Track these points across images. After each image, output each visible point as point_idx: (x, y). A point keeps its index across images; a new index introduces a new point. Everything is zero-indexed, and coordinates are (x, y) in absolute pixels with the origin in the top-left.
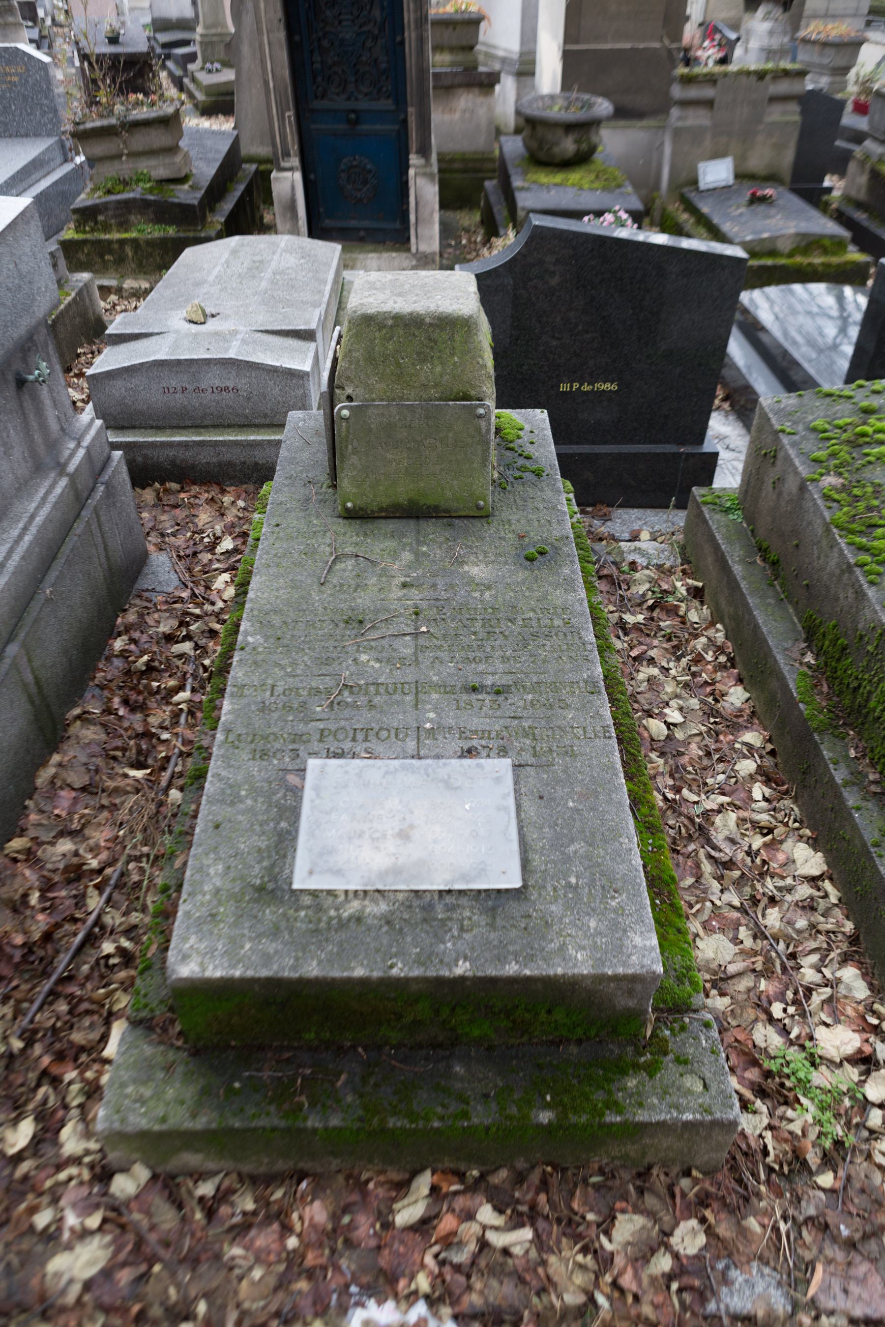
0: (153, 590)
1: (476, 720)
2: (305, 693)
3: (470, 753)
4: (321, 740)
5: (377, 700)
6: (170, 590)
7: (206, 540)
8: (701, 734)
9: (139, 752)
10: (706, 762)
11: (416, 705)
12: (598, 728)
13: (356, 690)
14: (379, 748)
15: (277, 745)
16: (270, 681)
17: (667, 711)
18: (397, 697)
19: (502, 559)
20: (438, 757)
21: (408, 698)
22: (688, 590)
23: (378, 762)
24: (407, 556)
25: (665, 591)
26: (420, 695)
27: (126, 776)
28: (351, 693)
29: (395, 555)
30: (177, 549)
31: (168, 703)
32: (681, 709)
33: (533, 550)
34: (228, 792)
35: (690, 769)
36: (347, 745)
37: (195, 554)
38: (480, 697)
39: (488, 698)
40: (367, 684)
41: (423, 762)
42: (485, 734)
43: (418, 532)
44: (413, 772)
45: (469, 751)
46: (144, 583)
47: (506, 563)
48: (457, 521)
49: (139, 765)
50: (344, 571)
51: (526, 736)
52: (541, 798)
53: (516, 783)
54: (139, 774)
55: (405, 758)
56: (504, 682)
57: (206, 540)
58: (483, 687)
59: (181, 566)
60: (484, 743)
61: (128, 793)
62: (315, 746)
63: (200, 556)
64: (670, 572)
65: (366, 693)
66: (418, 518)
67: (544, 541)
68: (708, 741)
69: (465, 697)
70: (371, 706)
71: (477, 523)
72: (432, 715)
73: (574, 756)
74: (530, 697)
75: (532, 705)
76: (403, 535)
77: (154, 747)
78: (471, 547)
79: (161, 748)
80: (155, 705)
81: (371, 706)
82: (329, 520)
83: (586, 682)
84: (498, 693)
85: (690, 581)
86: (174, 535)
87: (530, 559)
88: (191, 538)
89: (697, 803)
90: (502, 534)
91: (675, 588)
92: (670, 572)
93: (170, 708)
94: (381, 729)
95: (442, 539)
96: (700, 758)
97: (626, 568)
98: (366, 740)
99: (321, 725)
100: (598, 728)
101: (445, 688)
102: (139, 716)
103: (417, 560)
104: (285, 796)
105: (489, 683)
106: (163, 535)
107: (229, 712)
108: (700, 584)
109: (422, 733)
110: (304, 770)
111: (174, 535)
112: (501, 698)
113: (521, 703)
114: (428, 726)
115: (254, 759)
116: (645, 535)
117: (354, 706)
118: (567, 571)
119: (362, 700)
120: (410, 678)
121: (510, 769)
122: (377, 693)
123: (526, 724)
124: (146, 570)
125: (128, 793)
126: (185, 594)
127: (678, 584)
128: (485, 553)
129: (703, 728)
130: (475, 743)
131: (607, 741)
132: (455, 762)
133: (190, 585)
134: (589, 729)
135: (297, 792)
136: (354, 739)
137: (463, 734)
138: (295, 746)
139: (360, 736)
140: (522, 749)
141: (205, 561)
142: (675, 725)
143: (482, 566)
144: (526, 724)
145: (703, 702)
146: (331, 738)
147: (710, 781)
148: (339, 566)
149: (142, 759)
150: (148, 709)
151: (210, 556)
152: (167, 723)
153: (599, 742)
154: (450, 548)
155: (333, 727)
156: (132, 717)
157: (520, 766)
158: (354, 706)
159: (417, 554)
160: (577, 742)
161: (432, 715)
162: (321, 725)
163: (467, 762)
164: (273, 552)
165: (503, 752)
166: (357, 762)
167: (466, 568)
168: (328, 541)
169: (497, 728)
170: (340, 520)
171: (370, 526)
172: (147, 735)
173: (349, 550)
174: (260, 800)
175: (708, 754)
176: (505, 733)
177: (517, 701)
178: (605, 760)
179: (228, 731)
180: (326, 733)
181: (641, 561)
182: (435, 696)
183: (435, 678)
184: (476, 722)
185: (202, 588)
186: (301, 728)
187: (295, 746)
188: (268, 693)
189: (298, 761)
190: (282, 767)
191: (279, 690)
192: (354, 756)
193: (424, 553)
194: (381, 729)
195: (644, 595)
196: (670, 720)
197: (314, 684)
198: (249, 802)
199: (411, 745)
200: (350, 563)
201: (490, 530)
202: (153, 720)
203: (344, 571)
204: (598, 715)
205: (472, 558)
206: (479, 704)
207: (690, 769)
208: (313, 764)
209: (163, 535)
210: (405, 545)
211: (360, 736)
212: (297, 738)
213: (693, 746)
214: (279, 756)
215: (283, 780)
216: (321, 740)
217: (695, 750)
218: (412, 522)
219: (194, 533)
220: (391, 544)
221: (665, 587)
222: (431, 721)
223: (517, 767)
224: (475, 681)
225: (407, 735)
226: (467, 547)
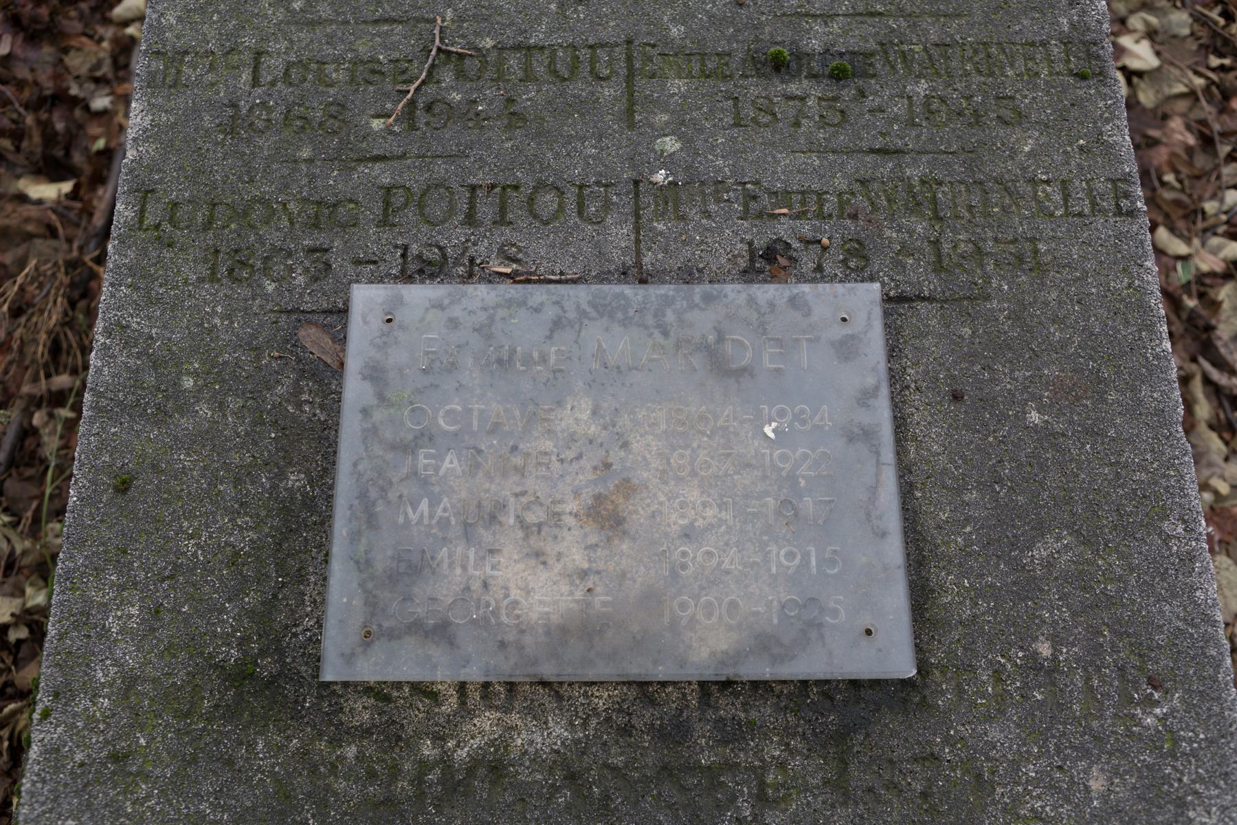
1: (784, 160)
2: (340, 76)
3: (768, 262)
4: (384, 222)
5: (529, 96)
8: (1192, 94)
9: (49, 137)
10: (1201, 161)
11: (630, 112)
12: (1101, 186)
13: (472, 65)
14: (539, 249)
15: (274, 237)
16: (249, 41)
17: (1126, 41)
18: (579, 88)
20: (689, 275)
21: (608, 92)
23: (538, 294)
26: (640, 82)
27: (22, 198)
28: (461, 75)
31: (107, 21)
32: (1150, 34)
34: (150, 379)
35: (1169, 178)
36: (454, 236)
38: (793, 88)
39: (815, 91)
40: (500, 48)
41: (656, 292)
42: (806, 202)
44: (625, 323)
45: (770, 255)
49: (52, 170)
51: (915, 207)
52: (957, 397)
53: (893, 351)
54: (47, 191)
55: (603, 278)
56: (854, 43)
58: (799, 56)
60: (806, 229)
61: (30, 237)
62: (372, 239)
65: (500, 77)
68: (1207, 110)
69: (754, 88)
70: (514, 118)
72: (670, 144)
73: (1039, 269)
74: (922, 87)
75: (930, 113)
77: (81, 127)
79: (94, 129)
80: (77, 26)
81: (514, 118)
83: (1066, 42)
84: (838, 76)
89: (1185, 258)
93: (109, 33)
94: (540, 186)
96: (1189, 150)
98: (502, 220)
99: (383, 175)
100: (1101, 186)
101: (703, 62)
102: (47, 52)
104: (297, 390)
105: (815, 45)
107: (146, 136)
109: (646, 199)
110: (344, 312)
112: (848, 93)
113: (899, 108)
114: (660, 176)
115: (213, 278)
117: (467, 114)
119: (489, 98)
120: (611, 31)
121: (877, 312)
122: (528, 76)
123: (914, 173)
125: (30, 237)
129: (1199, 82)
130: (783, 230)
131: (1124, 225)
132: (735, 292)
134: (1079, 185)
135: (325, 378)
136: (471, 219)
137: (754, 205)
138: (321, 239)
139: (486, 210)
140: (905, 250)
142: (1140, 74)
144: (914, 173)
145: (1199, 19)
146: (411, 214)
147: (1210, 206)
149: (59, 153)
150: (63, 35)
152: (106, 69)
153: (1105, 227)
155: (415, 180)
156: (32, 54)
157: (901, 299)
158: (467, 114)
160: (1046, 227)
161: (670, 144)
162: (383, 175)
163: (766, 292)
165: (857, 262)
166: (481, 293)
169: (840, 183)
172: (61, 99)
174: (234, 403)
175: (1207, 142)
176: (860, 201)
177: (892, 99)
178: (1121, 284)
179: (144, 194)
180: (398, 199)
182: (677, 86)
183: (676, 31)
184: (786, 167)
186: (333, 181)
187: (321, 239)
188: (246, 76)
189: (328, 284)
190: (286, 302)
191: (274, 65)
192: (473, 272)
194: (540, 186)
196: (1134, 64)
197: (362, 49)
198: (204, 410)
199: (619, 234)
202: (76, 62)
204: (1100, 146)
206: (791, 108)
207: (1169, 178)
208: (366, 298)
211: (486, 210)
212: (325, 213)
213: (1176, 124)
214: (278, 269)
215: (291, 343)
216: (384, 222)
217: (1179, 133)
222: (668, 161)
223: (894, 302)
224: (777, 37)
225: (607, 206)
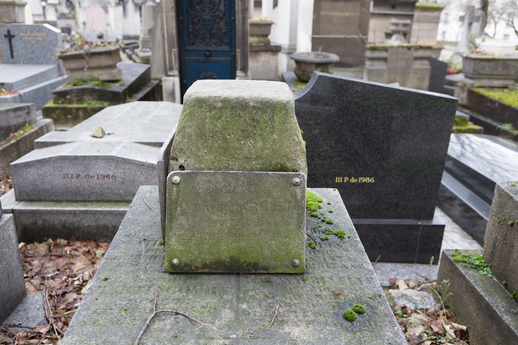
0: (20, 326)
6: (34, 325)
7: (76, 283)
19: (322, 319)
22: (455, 332)
24: (227, 314)
25: (437, 334)
29: (215, 312)
30: (52, 289)
33: (350, 310)
37: (64, 294)
43: (239, 288)
46: (14, 319)
47: (326, 324)
48: (274, 278)
50: (162, 330)
57: (76, 283)
59: (50, 304)
63: (67, 296)
64: (435, 316)
66: (238, 274)
67: (359, 299)
71: (293, 279)
76: (224, 291)
78: (290, 305)
82: (156, 275)
85: (455, 325)
86: (53, 278)
87: (349, 319)
88: (65, 281)
90: (319, 292)
91: (445, 331)
92: (435, 316)
95: (261, 296)
97: (399, 312)
103: (237, 319)
106: (43, 278)
108: (464, 328)
111: (53, 278)
116: (401, 283)
118: (389, 334)
124: (20, 308)
126: (44, 330)
127: (447, 327)
128: (304, 311)
133: (52, 321)
141: (70, 300)
143: (303, 327)
148: (158, 325)
151: (75, 296)
154: (270, 306)
159: (237, 312)
164: (94, 308)
167: (287, 329)
168: (151, 296)
170: (166, 276)
171: (193, 282)
173: (170, 306)
181: (410, 306)
185: (60, 324)
193: (244, 311)
195: (420, 337)
200: (169, 321)
201: (306, 288)
203: (162, 330)
205: (292, 317)
209: (43, 278)
210: (225, 302)
218: (233, 279)
219: (69, 276)
220: (212, 300)
221: (436, 329)
226: (286, 305)
